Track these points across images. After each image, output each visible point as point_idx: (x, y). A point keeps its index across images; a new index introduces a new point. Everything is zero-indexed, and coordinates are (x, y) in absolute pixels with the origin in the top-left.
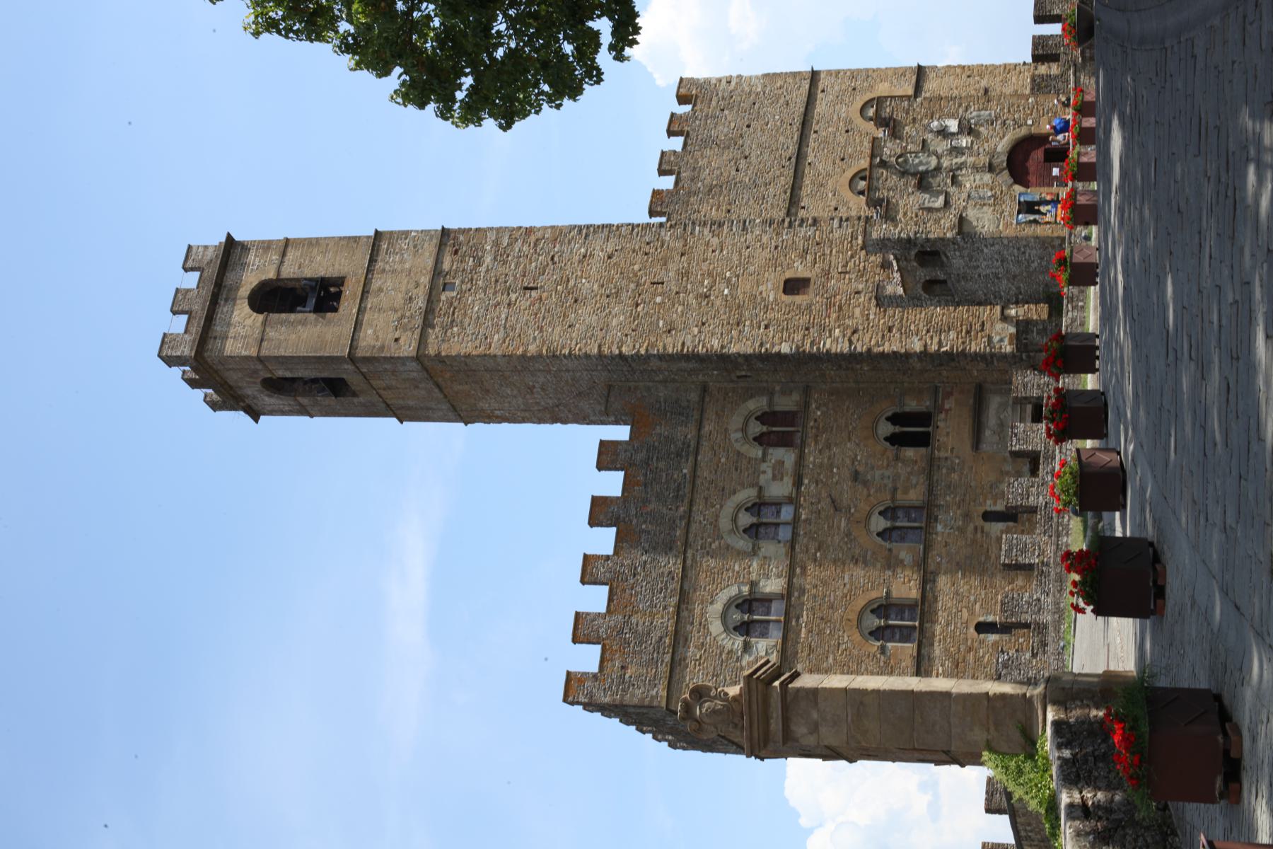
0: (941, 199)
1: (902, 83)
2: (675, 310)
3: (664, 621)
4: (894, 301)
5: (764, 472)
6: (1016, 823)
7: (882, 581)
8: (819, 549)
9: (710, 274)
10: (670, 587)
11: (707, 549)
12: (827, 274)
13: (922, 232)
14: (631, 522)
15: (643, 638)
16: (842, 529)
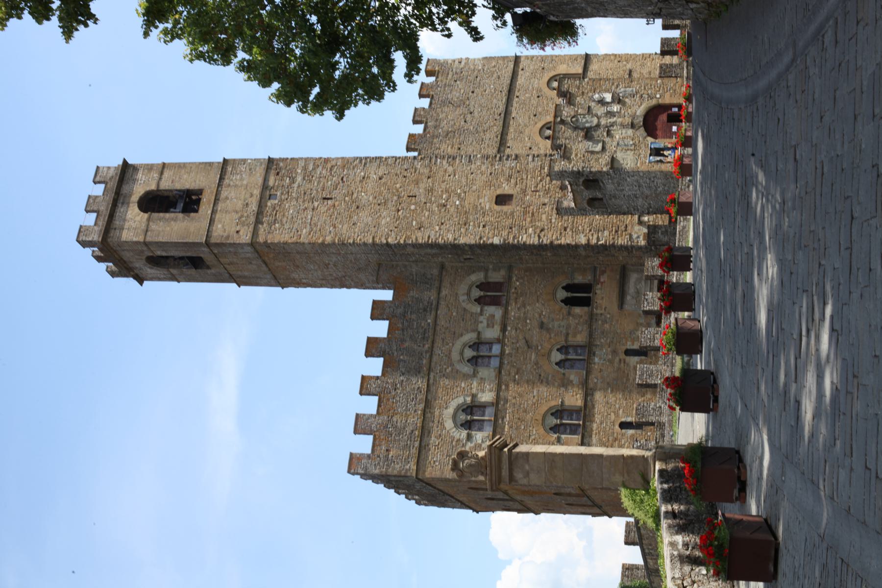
0: (599, 147)
1: (575, 65)
2: (423, 214)
3: (415, 420)
4: (569, 211)
5: (481, 322)
6: (643, 544)
8: (517, 373)
9: (447, 191)
10: (419, 397)
11: (444, 372)
12: (524, 192)
13: (587, 167)
14: (393, 354)
15: (400, 431)
16: (532, 360)
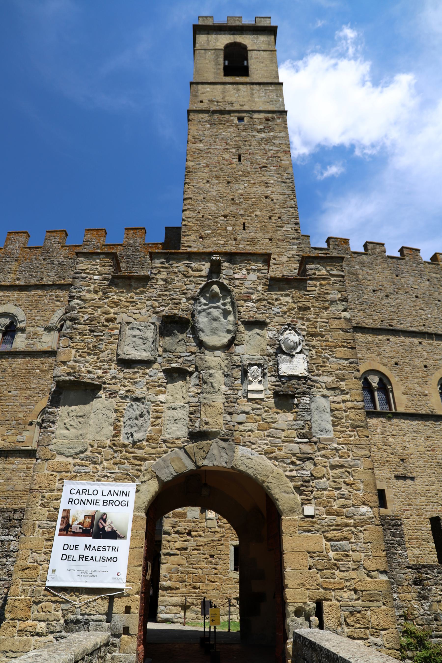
7: (7, 418)
8: (42, 371)
